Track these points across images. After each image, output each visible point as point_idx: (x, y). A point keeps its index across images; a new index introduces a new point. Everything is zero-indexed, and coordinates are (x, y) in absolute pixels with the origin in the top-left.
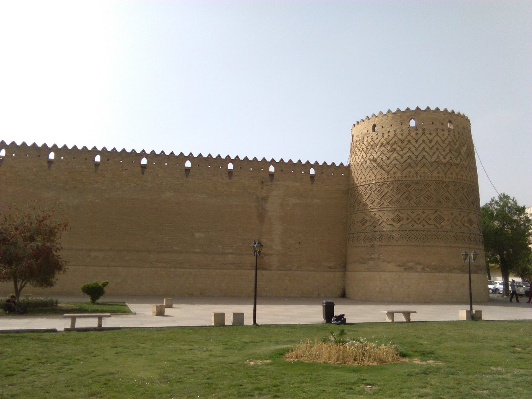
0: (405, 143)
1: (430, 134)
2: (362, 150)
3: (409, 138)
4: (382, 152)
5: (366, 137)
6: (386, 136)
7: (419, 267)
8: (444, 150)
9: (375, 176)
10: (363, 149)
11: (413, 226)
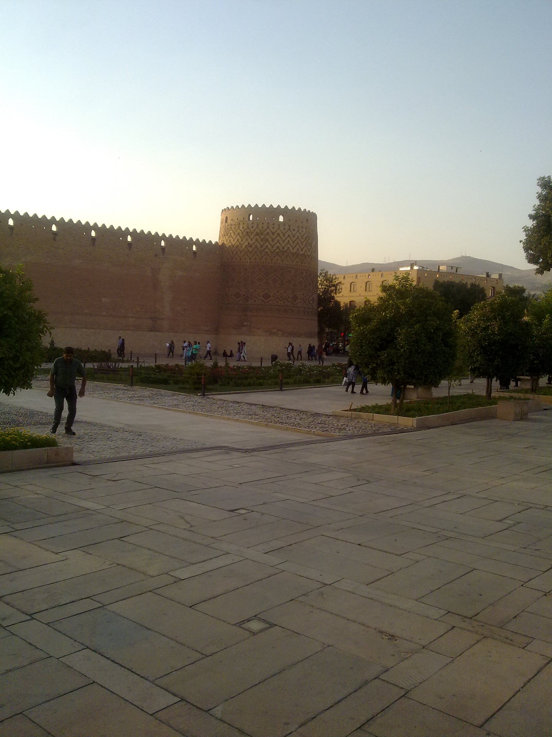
0: (276, 235)
1: (294, 230)
2: (237, 234)
3: (279, 231)
4: (257, 240)
5: (241, 224)
6: (260, 227)
7: (280, 333)
8: (302, 244)
9: (250, 259)
10: (239, 233)
11: (277, 302)
